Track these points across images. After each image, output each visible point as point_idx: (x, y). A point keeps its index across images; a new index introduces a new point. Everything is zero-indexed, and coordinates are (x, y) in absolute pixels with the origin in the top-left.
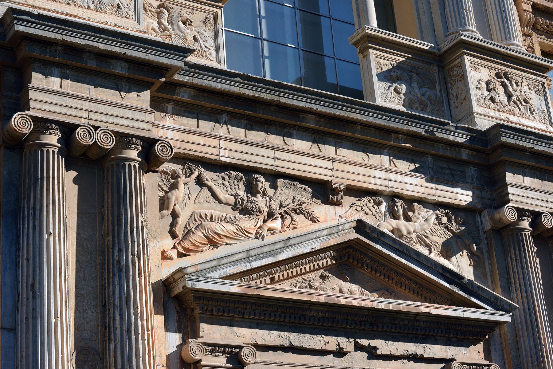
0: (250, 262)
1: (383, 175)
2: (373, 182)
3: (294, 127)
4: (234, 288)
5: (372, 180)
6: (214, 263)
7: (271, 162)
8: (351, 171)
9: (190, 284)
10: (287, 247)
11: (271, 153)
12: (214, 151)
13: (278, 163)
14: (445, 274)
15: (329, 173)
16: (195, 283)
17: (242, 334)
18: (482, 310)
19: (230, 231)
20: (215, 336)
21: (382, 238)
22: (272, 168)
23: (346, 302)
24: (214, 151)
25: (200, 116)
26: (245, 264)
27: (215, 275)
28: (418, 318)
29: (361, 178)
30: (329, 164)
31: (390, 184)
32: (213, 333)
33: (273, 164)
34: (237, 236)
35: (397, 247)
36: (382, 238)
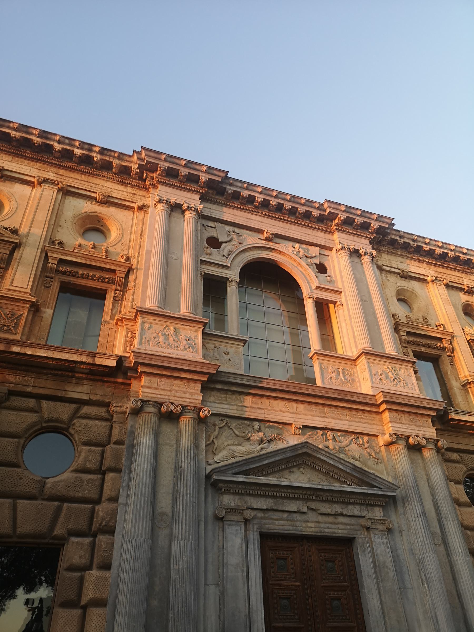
20: (232, 504)
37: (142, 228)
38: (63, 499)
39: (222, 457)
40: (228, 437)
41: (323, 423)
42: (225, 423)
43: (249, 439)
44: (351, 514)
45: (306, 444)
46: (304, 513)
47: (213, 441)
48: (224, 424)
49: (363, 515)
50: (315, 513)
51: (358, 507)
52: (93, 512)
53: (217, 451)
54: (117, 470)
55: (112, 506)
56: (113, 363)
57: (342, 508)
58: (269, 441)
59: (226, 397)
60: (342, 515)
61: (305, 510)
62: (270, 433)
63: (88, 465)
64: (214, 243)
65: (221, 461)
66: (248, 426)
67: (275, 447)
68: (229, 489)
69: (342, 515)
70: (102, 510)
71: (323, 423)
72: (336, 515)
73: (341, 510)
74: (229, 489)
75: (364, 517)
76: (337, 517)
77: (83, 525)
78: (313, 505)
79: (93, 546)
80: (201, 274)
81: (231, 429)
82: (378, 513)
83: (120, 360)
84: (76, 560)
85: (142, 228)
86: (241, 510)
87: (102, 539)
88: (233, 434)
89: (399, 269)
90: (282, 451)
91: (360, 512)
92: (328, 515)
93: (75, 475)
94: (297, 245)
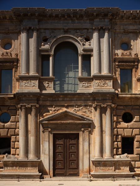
37: (20, 40)
38: (9, 129)
52: (15, 131)
54: (19, 122)
55: (18, 129)
56: (13, 96)
62: (57, 108)
63: (13, 121)
64: (45, 40)
70: (17, 130)
77: (13, 133)
79: (16, 137)
80: (40, 55)
83: (14, 95)
84: (13, 140)
85: (20, 40)
87: (17, 136)
89: (124, 29)
93: (10, 123)
94: (78, 31)
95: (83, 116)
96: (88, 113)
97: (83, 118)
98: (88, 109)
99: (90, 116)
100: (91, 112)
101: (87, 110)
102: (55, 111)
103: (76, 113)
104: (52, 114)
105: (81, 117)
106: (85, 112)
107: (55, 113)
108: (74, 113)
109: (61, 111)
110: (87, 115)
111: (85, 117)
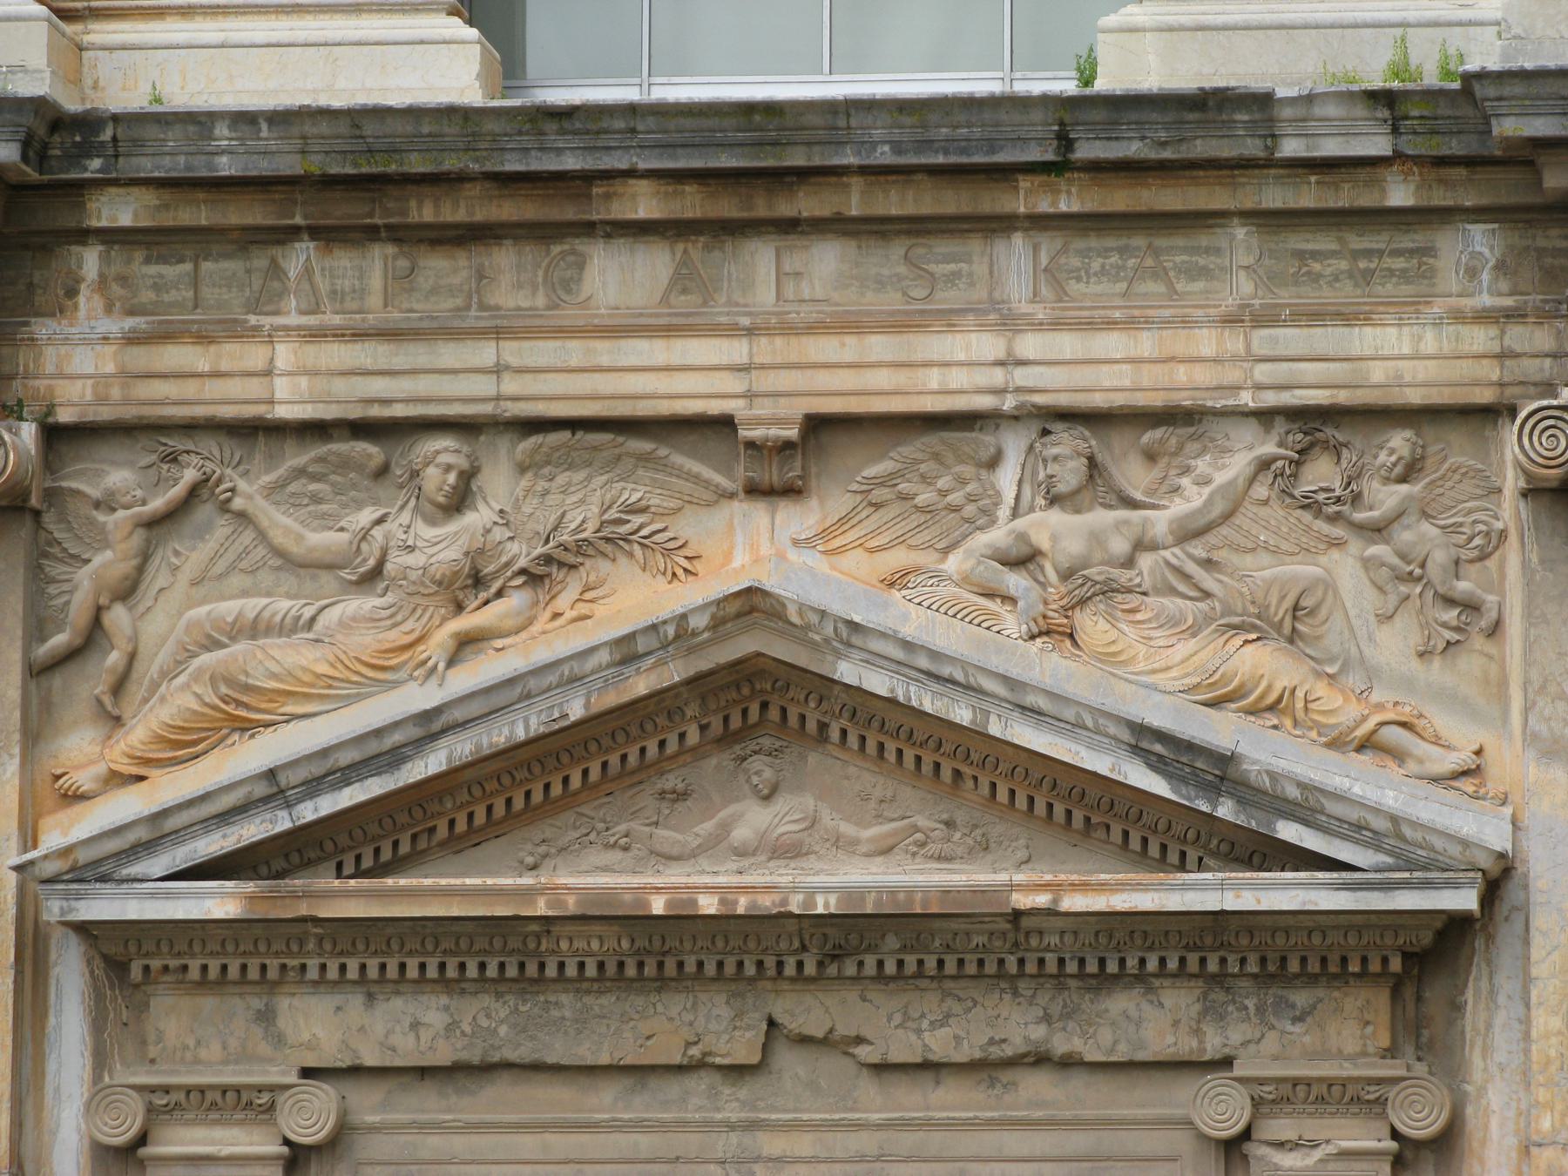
0: (289, 805)
1: (989, 345)
2: (934, 385)
3: (588, 229)
4: (219, 902)
5: (934, 379)
6: (142, 834)
7: (484, 386)
8: (834, 358)
9: (56, 910)
10: (433, 737)
11: (485, 353)
12: (254, 388)
13: (510, 385)
14: (1145, 744)
15: (735, 384)
16: (73, 903)
17: (306, 1036)
18: (1344, 874)
19: (300, 674)
20: (203, 1053)
21: (856, 640)
22: (487, 409)
23: (668, 904)
24: (254, 388)
25: (7, 369)
26: (268, 816)
27: (160, 864)
28: (1025, 922)
29: (882, 379)
30: (736, 350)
31: (1022, 377)
32: (198, 1043)
33: (492, 392)
34: (330, 687)
35: (923, 662)
36: (856, 640)
39: (160, 739)
40: (220, 576)
41: (998, 377)
42: (190, 475)
43: (376, 573)
44: (1122, 1053)
45: (751, 605)
46: (738, 1071)
47: (96, 623)
48: (177, 491)
49: (1213, 1045)
50: (831, 1065)
51: (1180, 1000)
53: (136, 691)
57: (1047, 1019)
58: (532, 578)
59: (195, 283)
60: (1039, 1059)
61: (742, 1046)
65: (148, 762)
66: (383, 472)
67: (583, 609)
68: (174, 963)
69: (1039, 1059)
71: (998, 377)
72: (984, 1068)
73: (1038, 1032)
74: (174, 963)
75: (1226, 1063)
76: (1006, 1076)
78: (806, 1012)
81: (242, 515)
82: (1343, 1035)
86: (260, 1089)
88: (261, 551)
90: (552, 678)
91: (1197, 1032)
92: (929, 1068)
95: (1221, 731)
96: (1393, 646)
97: (1200, 808)
98: (1377, 530)
99: (1441, 721)
100: (1471, 606)
101: (1346, 571)
102: (473, 580)
103: (1047, 667)
104: (380, 672)
105: (1157, 764)
106: (1293, 624)
107: (467, 643)
108: (1004, 646)
109: (633, 598)
110: (1339, 707)
111: (1266, 751)
